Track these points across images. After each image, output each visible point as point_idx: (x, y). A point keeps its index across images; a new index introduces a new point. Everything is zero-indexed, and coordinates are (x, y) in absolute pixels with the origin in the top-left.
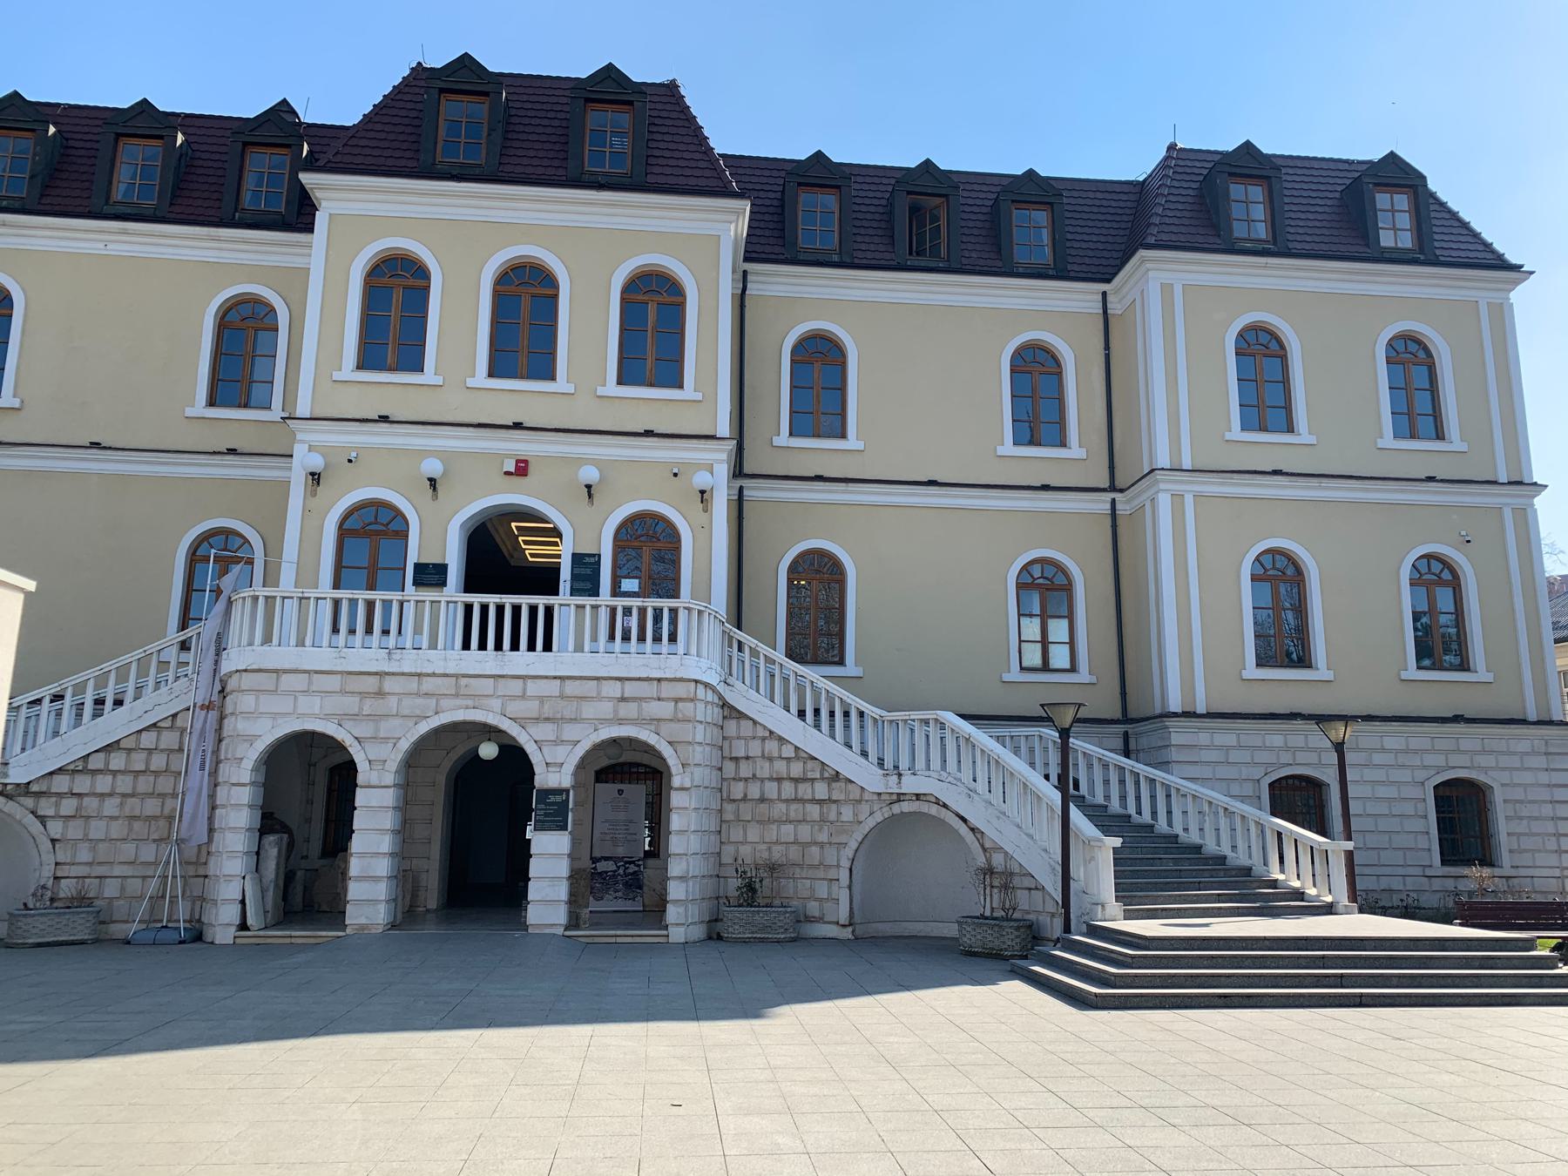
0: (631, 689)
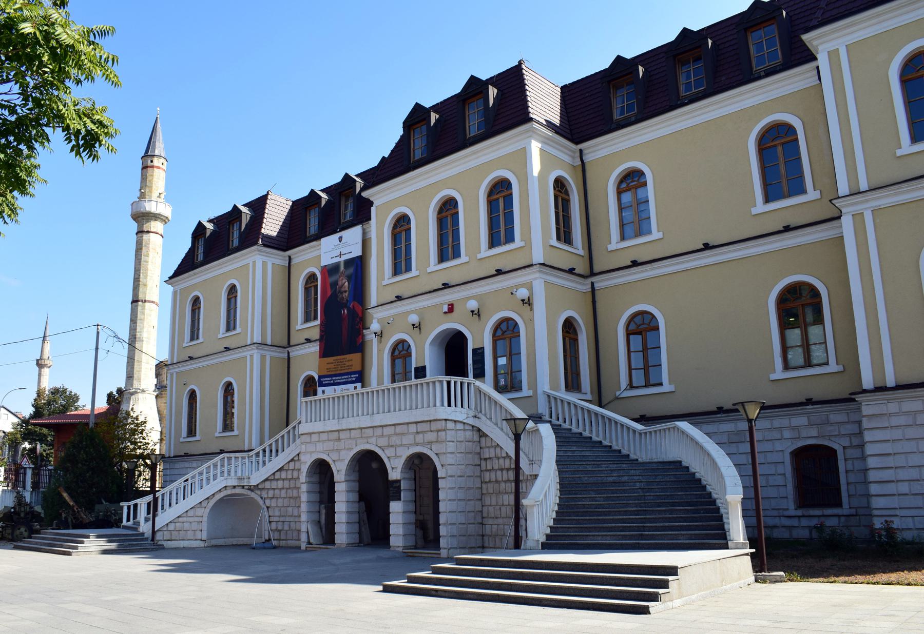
0: (421, 427)
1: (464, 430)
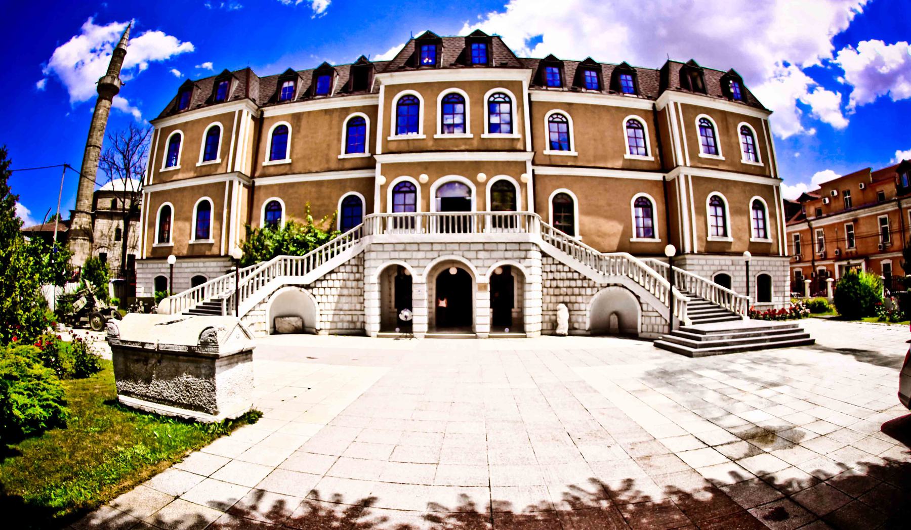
0: (509, 247)
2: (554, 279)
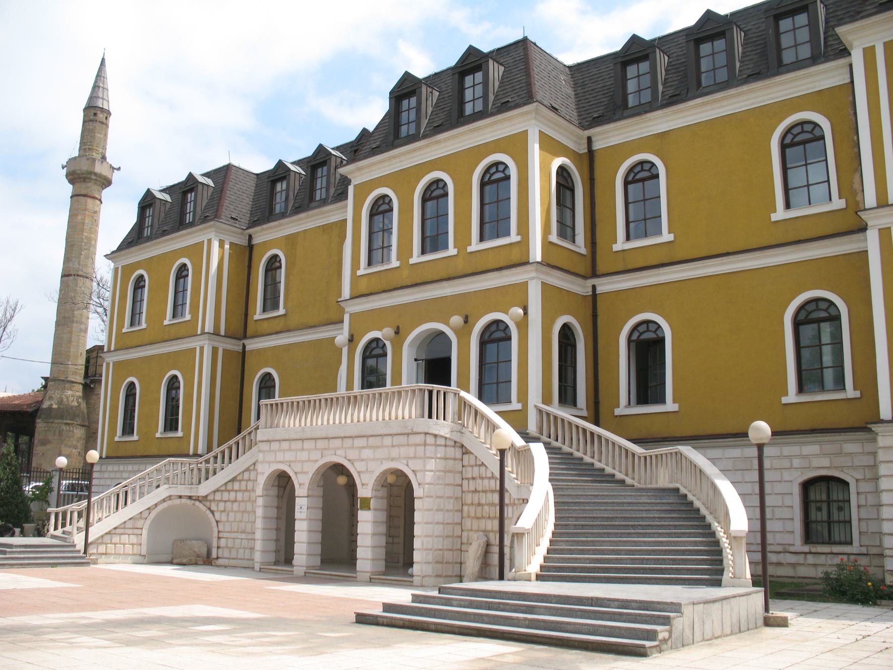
1: (446, 446)
2: (476, 491)
